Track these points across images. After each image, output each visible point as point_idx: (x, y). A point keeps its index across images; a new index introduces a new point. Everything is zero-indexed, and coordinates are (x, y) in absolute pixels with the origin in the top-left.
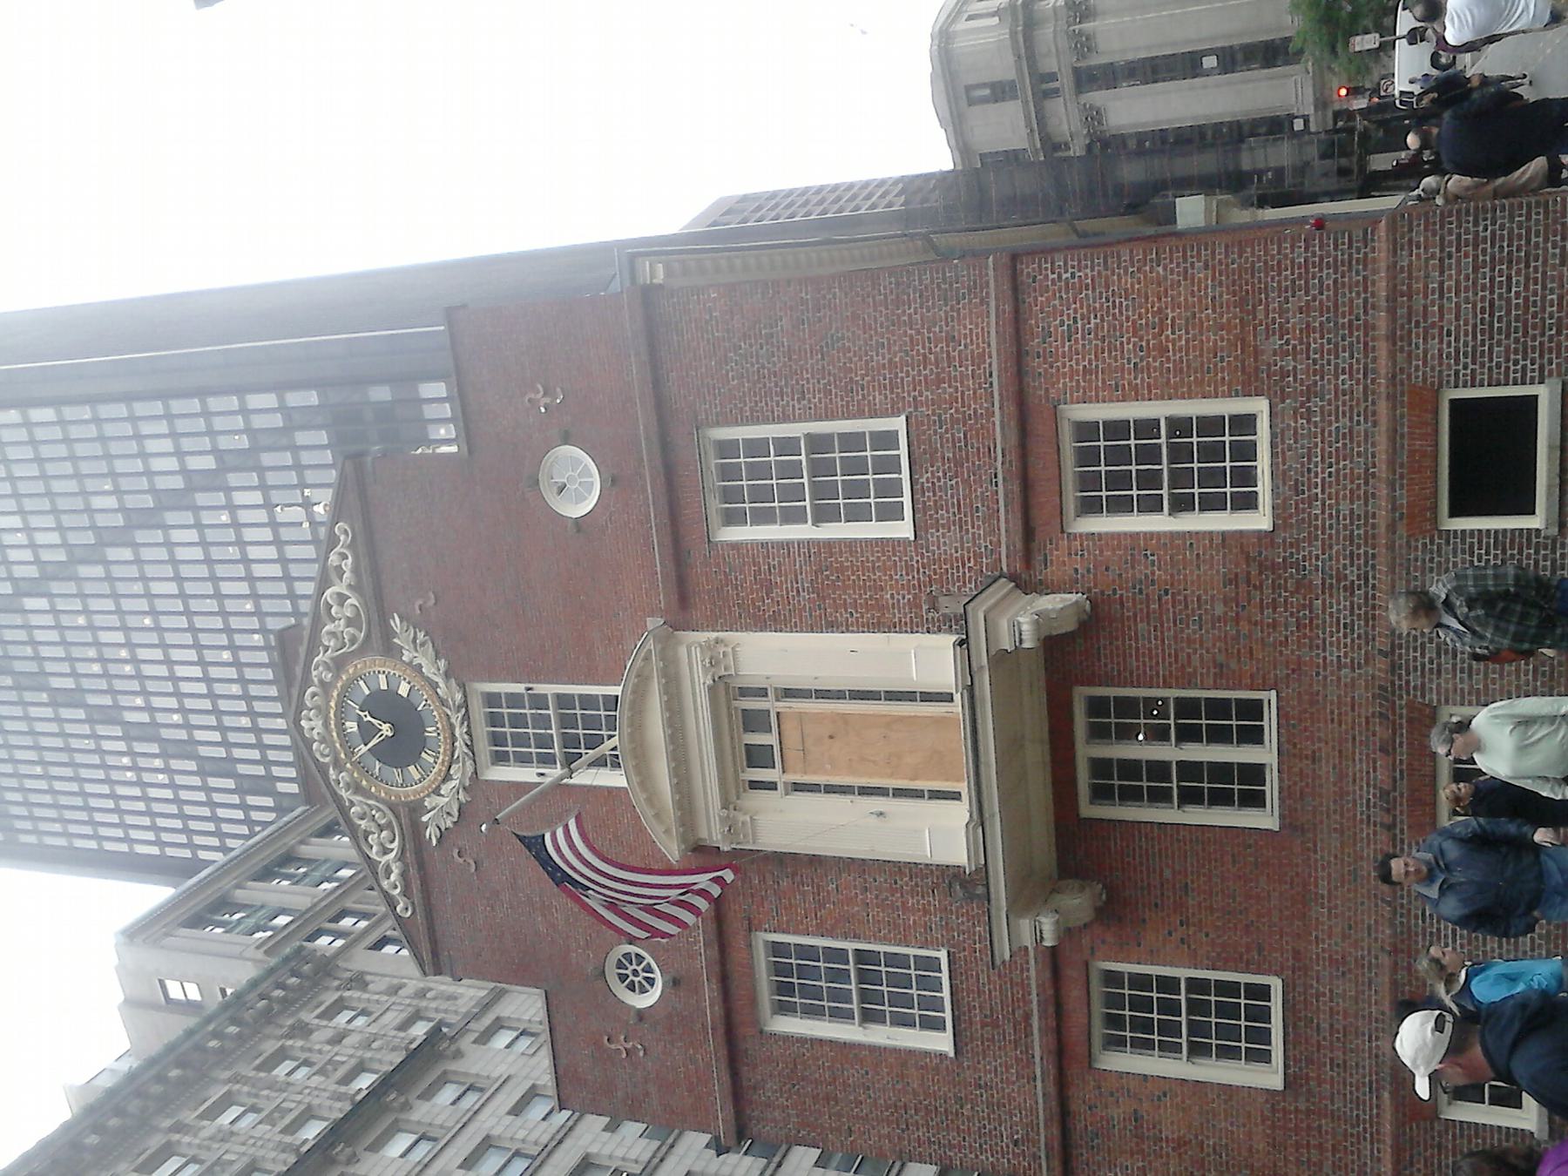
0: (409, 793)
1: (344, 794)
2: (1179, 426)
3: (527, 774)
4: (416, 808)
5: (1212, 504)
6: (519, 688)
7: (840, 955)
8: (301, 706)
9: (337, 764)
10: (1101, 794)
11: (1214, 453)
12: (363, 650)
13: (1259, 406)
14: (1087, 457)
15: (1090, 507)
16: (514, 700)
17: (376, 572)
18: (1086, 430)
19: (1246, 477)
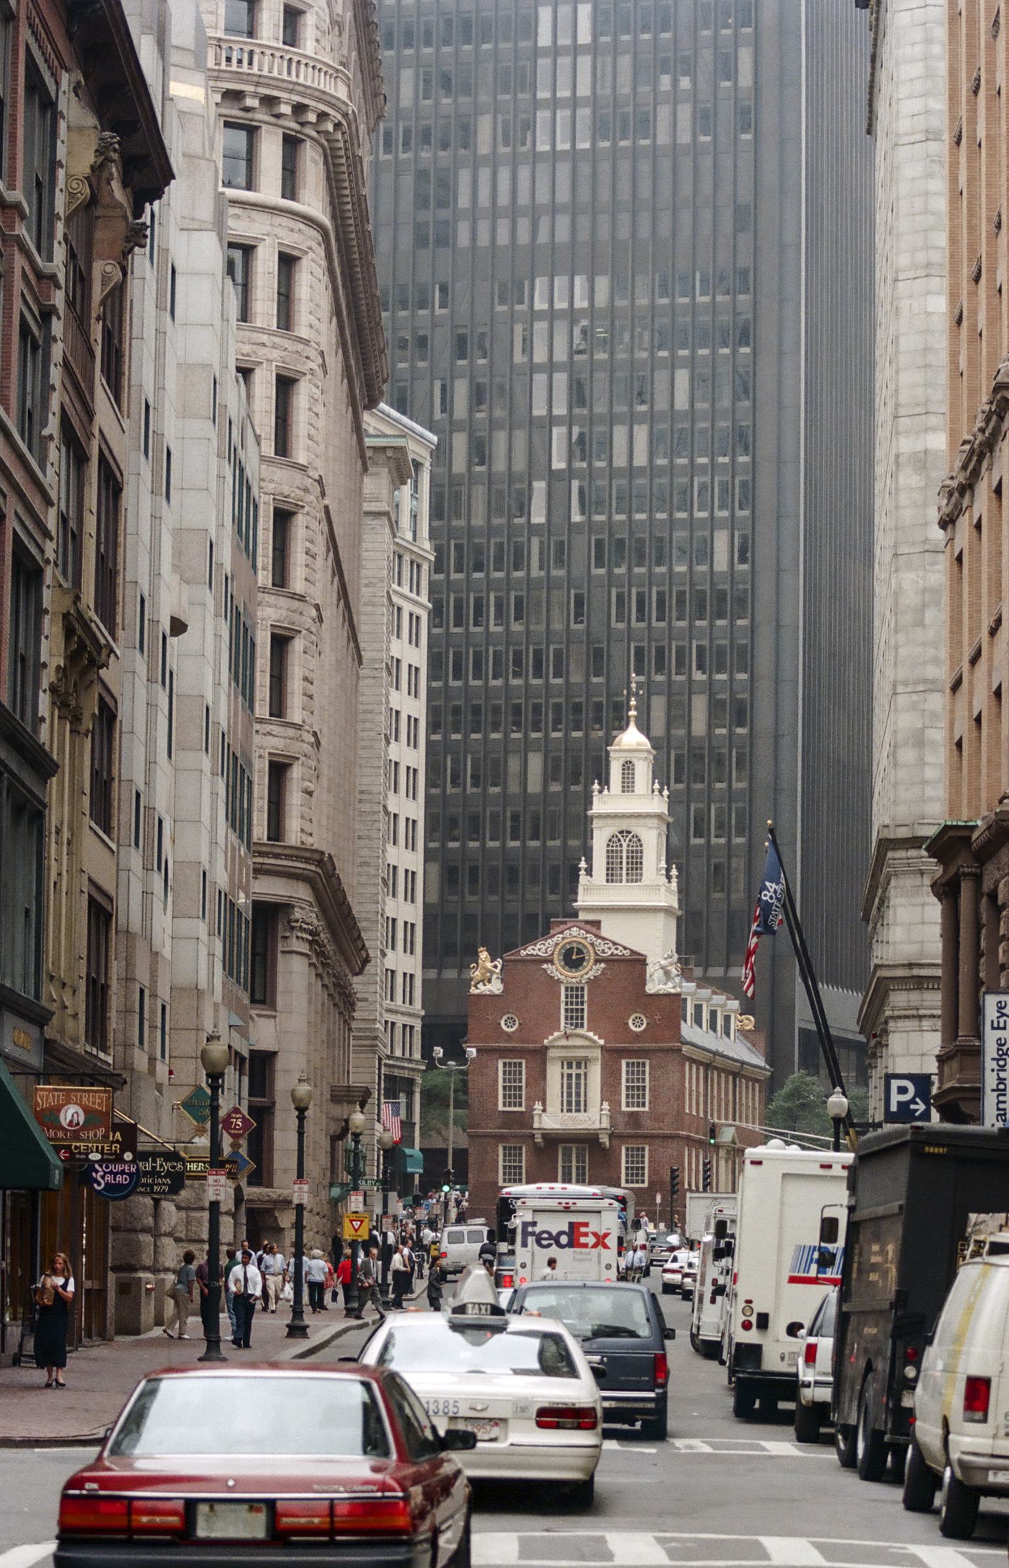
0: (556, 961)
1: (555, 939)
2: (643, 1168)
3: (563, 998)
4: (551, 962)
5: (627, 1175)
6: (586, 998)
7: (520, 1081)
8: (581, 929)
9: (563, 938)
10: (564, 1149)
11: (637, 1175)
12: (596, 954)
13: (646, 1185)
14: (638, 1149)
15: (627, 1149)
16: (583, 996)
17: (617, 960)
18: (643, 1149)
19: (632, 1182)
